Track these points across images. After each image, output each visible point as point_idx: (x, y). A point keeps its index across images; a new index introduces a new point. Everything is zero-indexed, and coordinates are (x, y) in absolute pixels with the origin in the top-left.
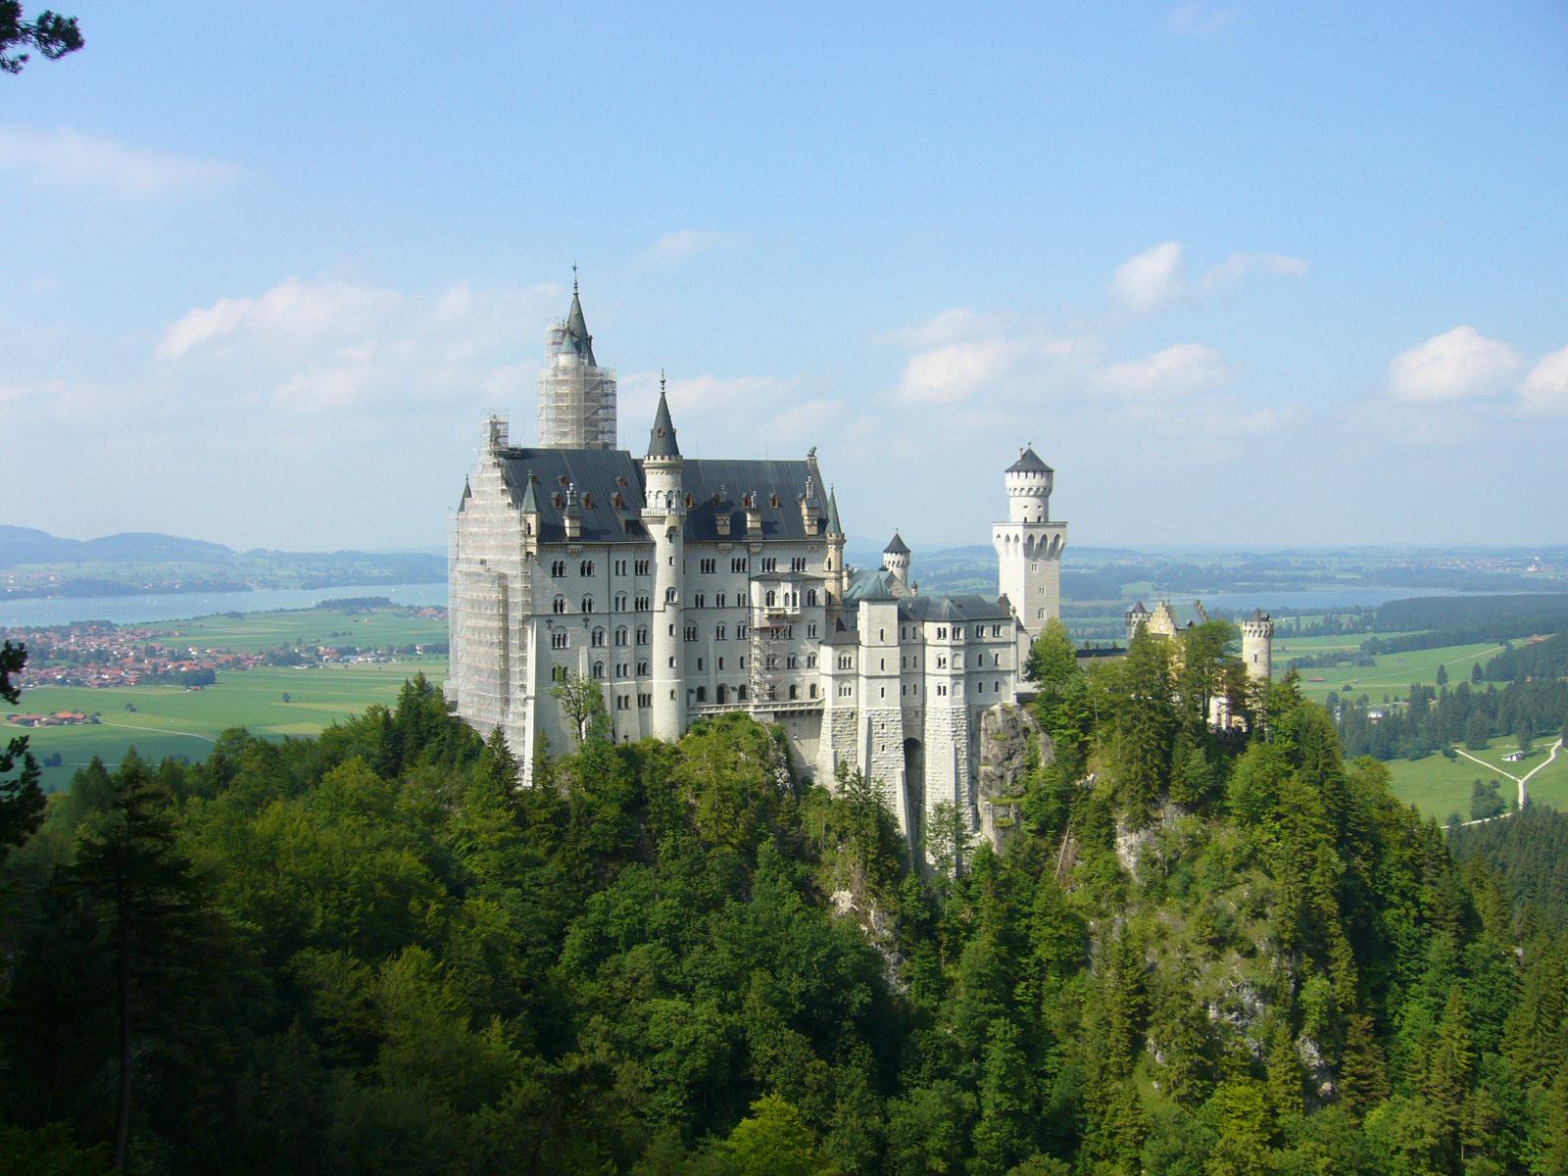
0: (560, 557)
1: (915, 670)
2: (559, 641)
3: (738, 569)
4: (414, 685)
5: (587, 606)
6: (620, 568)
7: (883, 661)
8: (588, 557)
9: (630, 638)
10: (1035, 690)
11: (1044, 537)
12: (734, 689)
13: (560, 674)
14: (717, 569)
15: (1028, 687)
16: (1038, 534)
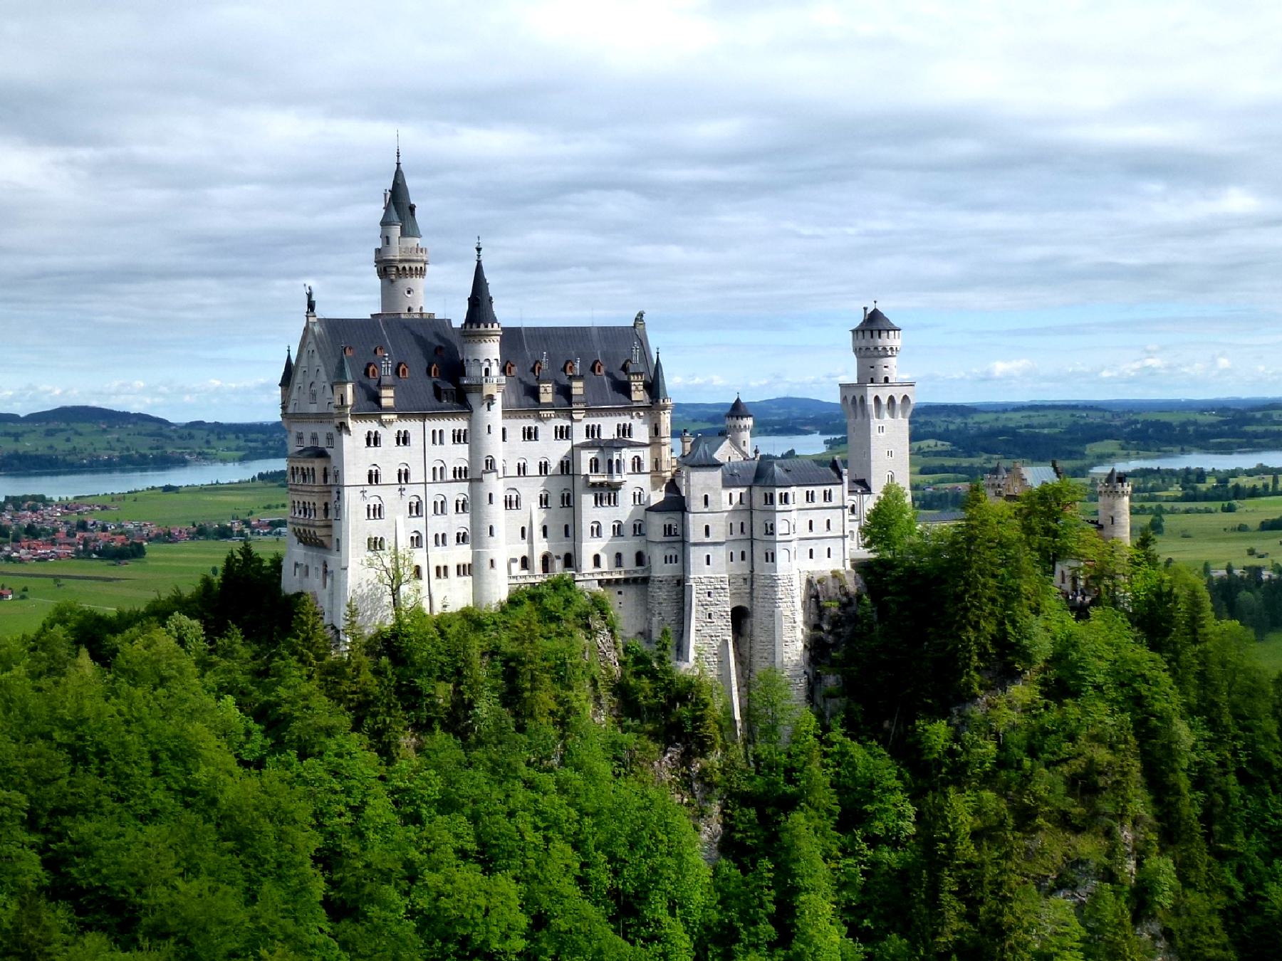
0: (373, 426)
1: (742, 537)
2: (376, 512)
3: (561, 437)
4: (239, 557)
5: (404, 476)
6: (438, 437)
7: (707, 528)
8: (404, 425)
9: (451, 507)
10: (873, 556)
11: (891, 399)
12: (558, 558)
13: (375, 544)
14: (540, 437)
15: (865, 554)
16: (884, 395)
